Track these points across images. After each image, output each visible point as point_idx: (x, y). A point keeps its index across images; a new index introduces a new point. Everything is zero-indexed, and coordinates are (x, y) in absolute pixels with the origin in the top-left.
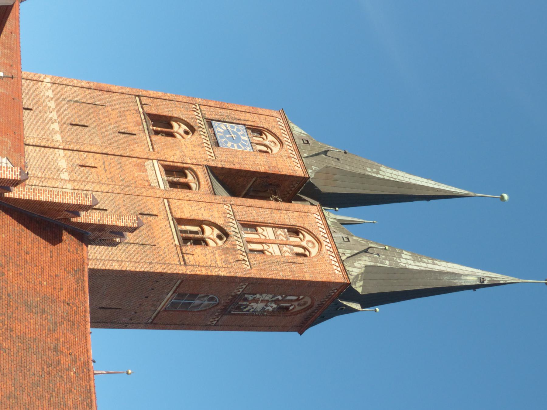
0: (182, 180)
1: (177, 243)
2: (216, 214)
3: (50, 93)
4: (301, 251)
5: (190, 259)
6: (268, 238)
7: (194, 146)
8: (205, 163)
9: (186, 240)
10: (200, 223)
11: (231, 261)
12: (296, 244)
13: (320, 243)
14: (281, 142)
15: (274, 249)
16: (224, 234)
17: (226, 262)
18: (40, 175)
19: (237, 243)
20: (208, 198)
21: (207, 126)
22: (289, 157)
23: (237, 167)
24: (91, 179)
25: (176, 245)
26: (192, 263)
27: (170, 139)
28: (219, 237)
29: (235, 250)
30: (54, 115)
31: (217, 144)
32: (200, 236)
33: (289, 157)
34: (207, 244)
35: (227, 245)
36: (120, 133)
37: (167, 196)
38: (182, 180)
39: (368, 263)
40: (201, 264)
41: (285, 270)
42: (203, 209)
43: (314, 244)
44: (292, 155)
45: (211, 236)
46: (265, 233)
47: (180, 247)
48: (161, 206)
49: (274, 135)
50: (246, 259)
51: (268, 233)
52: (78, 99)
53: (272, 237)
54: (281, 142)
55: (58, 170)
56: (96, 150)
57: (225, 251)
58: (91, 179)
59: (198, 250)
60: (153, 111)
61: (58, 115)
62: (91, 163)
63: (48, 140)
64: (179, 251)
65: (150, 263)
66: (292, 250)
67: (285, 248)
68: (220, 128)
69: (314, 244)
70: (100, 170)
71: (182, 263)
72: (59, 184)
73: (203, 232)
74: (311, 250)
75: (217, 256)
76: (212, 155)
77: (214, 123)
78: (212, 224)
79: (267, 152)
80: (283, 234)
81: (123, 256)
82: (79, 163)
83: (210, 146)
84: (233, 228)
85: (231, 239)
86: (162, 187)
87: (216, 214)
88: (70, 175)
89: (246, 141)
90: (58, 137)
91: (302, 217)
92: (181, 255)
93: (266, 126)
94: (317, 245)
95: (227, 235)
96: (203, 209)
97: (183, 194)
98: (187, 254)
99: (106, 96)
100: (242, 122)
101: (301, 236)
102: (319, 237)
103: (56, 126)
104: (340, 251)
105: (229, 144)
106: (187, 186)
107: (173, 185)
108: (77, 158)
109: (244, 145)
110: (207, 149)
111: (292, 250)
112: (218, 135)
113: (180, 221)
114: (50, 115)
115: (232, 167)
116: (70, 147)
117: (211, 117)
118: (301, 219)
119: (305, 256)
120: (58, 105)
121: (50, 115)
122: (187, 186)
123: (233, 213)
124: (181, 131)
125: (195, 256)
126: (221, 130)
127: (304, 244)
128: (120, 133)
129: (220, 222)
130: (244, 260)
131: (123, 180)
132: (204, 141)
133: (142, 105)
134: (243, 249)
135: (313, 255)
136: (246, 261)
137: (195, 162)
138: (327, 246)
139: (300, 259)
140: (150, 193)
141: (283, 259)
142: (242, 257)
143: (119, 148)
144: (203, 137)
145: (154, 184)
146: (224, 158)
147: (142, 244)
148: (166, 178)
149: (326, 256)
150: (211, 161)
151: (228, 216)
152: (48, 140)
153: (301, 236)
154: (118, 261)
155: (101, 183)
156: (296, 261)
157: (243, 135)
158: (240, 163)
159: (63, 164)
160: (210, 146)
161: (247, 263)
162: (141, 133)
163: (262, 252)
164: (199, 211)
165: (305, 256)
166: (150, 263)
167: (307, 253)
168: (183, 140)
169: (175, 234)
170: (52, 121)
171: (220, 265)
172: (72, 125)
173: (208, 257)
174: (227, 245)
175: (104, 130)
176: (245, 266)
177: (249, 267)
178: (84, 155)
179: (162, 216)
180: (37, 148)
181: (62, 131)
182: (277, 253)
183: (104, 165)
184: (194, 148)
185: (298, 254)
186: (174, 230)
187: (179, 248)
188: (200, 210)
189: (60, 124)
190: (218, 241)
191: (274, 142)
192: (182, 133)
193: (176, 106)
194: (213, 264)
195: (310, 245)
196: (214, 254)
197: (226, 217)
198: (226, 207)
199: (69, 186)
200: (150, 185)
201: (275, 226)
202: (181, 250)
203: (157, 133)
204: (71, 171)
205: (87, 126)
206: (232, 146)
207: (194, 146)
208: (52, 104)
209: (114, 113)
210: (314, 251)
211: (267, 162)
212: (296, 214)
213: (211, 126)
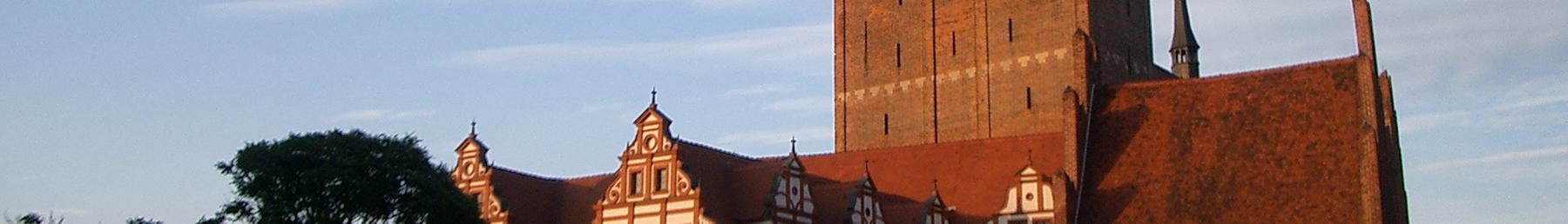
3: (860, 93)
18: (974, 103)
30: (890, 88)
55: (964, 80)
58: (971, 39)
62: (947, 39)
63: (925, 95)
70: (956, 27)
72: (984, 79)
88: (968, 66)
90: (920, 81)
99: (850, 21)
103: (905, 85)
108: (945, 57)
114: (890, 92)
121: (890, 92)
152: (925, 95)
159: (954, 75)
170: (898, 90)
175: (901, 24)
181: (911, 77)
204: (964, 65)
208: (874, 90)
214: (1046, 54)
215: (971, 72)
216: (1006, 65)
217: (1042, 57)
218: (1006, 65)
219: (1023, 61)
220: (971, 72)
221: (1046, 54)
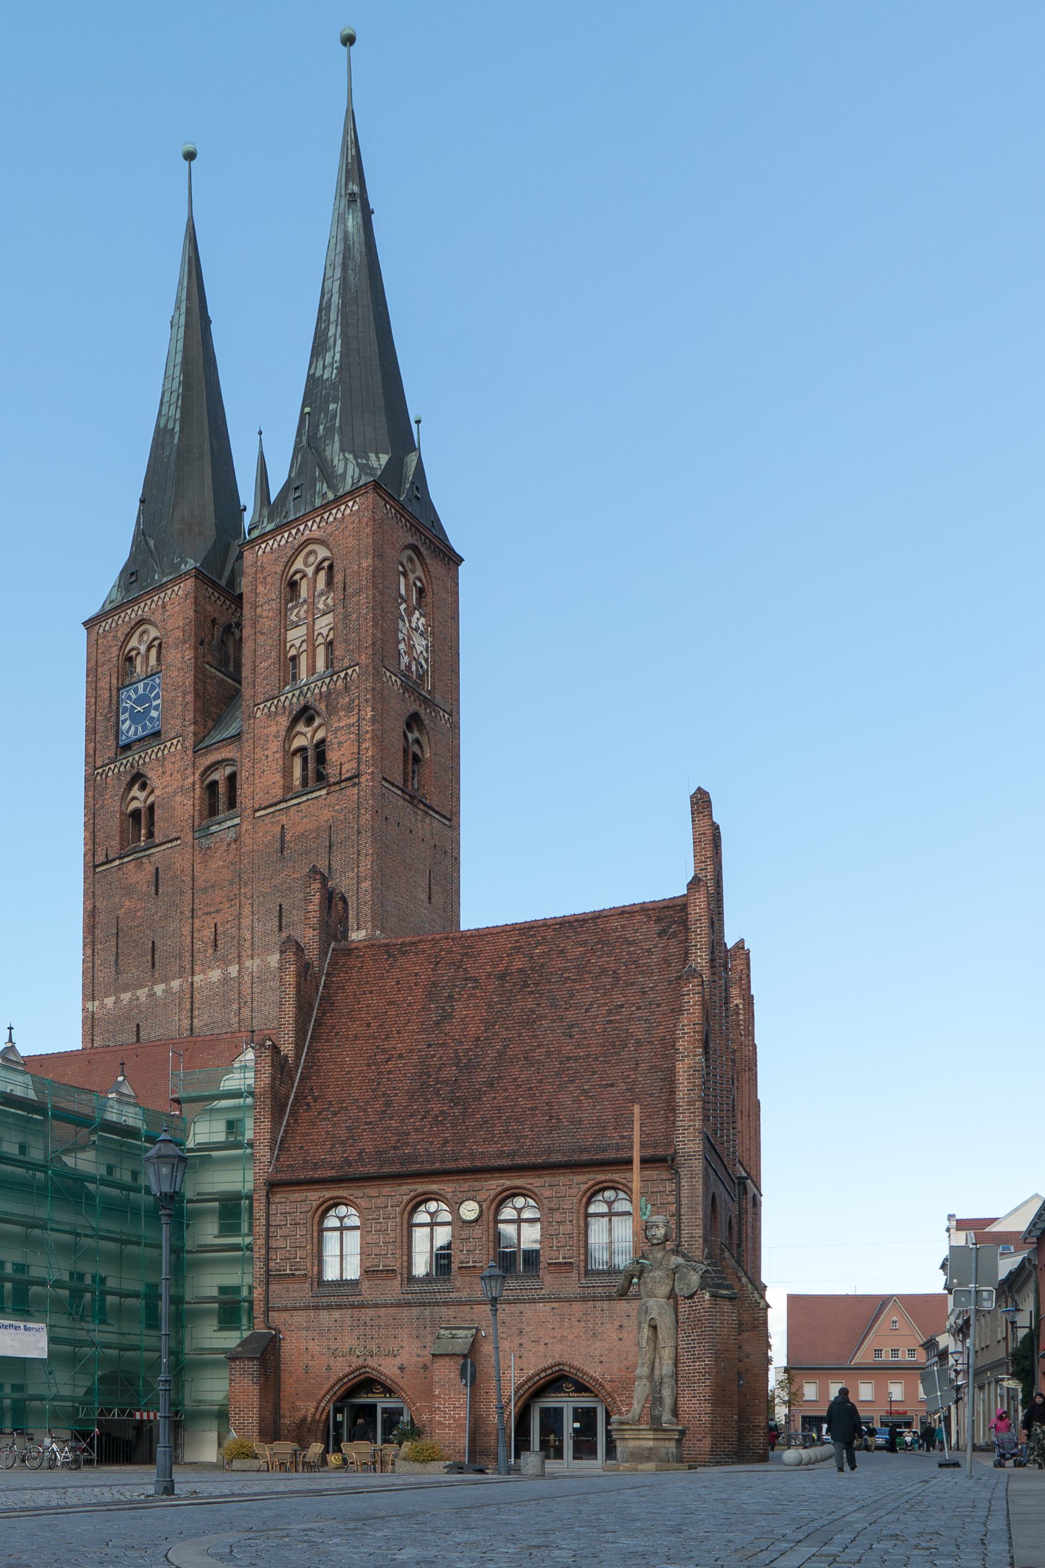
0: (222, 789)
1: (324, 792)
3: (109, 1001)
4: (322, 576)
6: (305, 637)
7: (164, 773)
8: (190, 752)
9: (321, 777)
10: (290, 754)
11: (347, 699)
12: (311, 585)
14: (141, 622)
15: (323, 624)
16: (305, 714)
17: (349, 708)
18: (235, 1007)
19: (317, 691)
20: (247, 746)
21: (129, 753)
23: (190, 698)
24: (234, 932)
25: (328, 794)
26: (355, 766)
27: (158, 812)
28: (310, 721)
30: (142, 993)
31: (157, 734)
32: (310, 753)
34: (323, 741)
35: (323, 706)
36: (157, 893)
37: (250, 811)
38: (222, 789)
39: (337, 445)
40: (356, 750)
41: (358, 603)
42: (266, 753)
43: (311, 553)
44: (160, 603)
45: (309, 736)
46: (297, 643)
47: (330, 786)
48: (267, 820)
49: (128, 636)
50: (342, 675)
51: (296, 636)
52: (113, 959)
53: (302, 631)
54: (141, 622)
55: (226, 980)
56: (186, 930)
57: (332, 710)
58: (234, 932)
59: (333, 756)
60: (115, 843)
61: (141, 986)
62: (208, 934)
63: (181, 998)
64: (337, 788)
66: (322, 594)
67: (321, 606)
68: (129, 730)
69: (311, 553)
70: (219, 918)
71: (356, 780)
73: (302, 749)
74: (319, 558)
75: (341, 724)
76: (175, 741)
77: (123, 740)
79: (160, 645)
80: (296, 611)
81: (350, 875)
82: (211, 951)
83: (162, 747)
84: (291, 699)
86: (237, 821)
87: (273, 729)
88: (231, 963)
89: (146, 686)
90: (175, 984)
91: (265, 578)
92: (343, 785)
93: (115, 651)
94: (310, 547)
95: (306, 709)
96: (266, 753)
97: (245, 786)
98: (340, 774)
99: (102, 918)
100: (114, 693)
101: (297, 577)
102: (297, 543)
103: (159, 989)
104: (318, 502)
105: (154, 714)
106: (232, 778)
109: (153, 688)
110: (166, 752)
111: (322, 594)
112: (141, 733)
113: (287, 788)
114: (143, 999)
115: (191, 707)
117: (113, 748)
118: (269, 579)
119: (331, 567)
120: (125, 991)
121: (143, 999)
122: (232, 778)
123: (268, 701)
124: (142, 795)
125: (344, 760)
126: (133, 729)
127: (310, 571)
128: (157, 893)
129: (284, 721)
130: (345, 678)
131: (232, 883)
132: (153, 756)
133: (108, 862)
134: (327, 680)
135: (329, 554)
136: (347, 674)
137: (190, 771)
138: (312, 529)
139: (338, 578)
140: (247, 839)
141: (340, 609)
142: (340, 682)
143: (182, 893)
144: (147, 759)
145: (232, 834)
146: (179, 722)
147: (330, 847)
148: (221, 816)
149: (330, 529)
150: (187, 744)
151: (273, 709)
152: (181, 998)
153: (297, 577)
154: (358, 883)
155: (239, 916)
156: (341, 585)
157: (136, 690)
158: (185, 693)
159: (215, 975)
160: (162, 747)
161: (350, 671)
162: (153, 859)
163: (330, 644)
164: (270, 759)
165: (331, 567)
166: (359, 833)
167: (326, 564)
168: (157, 792)
169: (310, 796)
170: (152, 995)
173: (343, 739)
174: (322, 707)
175: (156, 918)
176: (355, 674)
177: (357, 668)
178: (198, 945)
179: (284, 819)
180: (196, 1013)
181: (166, 980)
182: (329, 619)
183: (210, 913)
184: (168, 773)
185: (330, 582)
186: (304, 798)
187: (332, 788)
188: (267, 757)
189: (154, 984)
190: (316, 724)
191: (141, 635)
192: (145, 793)
193: (102, 807)
194: (354, 729)
195: (311, 559)
196: (337, 729)
197: (276, 712)
198: (259, 714)
199: (248, 963)
200: (235, 841)
201: (284, 625)
202: (335, 784)
203: (150, 835)
205: (153, 943)
206: (156, 708)
207: (164, 773)
208: (126, 997)
209: (127, 903)
210: (322, 552)
211: (176, 647)
212: (261, 589)
213: (127, 747)
215: (233, 970)
220: (233, 970)
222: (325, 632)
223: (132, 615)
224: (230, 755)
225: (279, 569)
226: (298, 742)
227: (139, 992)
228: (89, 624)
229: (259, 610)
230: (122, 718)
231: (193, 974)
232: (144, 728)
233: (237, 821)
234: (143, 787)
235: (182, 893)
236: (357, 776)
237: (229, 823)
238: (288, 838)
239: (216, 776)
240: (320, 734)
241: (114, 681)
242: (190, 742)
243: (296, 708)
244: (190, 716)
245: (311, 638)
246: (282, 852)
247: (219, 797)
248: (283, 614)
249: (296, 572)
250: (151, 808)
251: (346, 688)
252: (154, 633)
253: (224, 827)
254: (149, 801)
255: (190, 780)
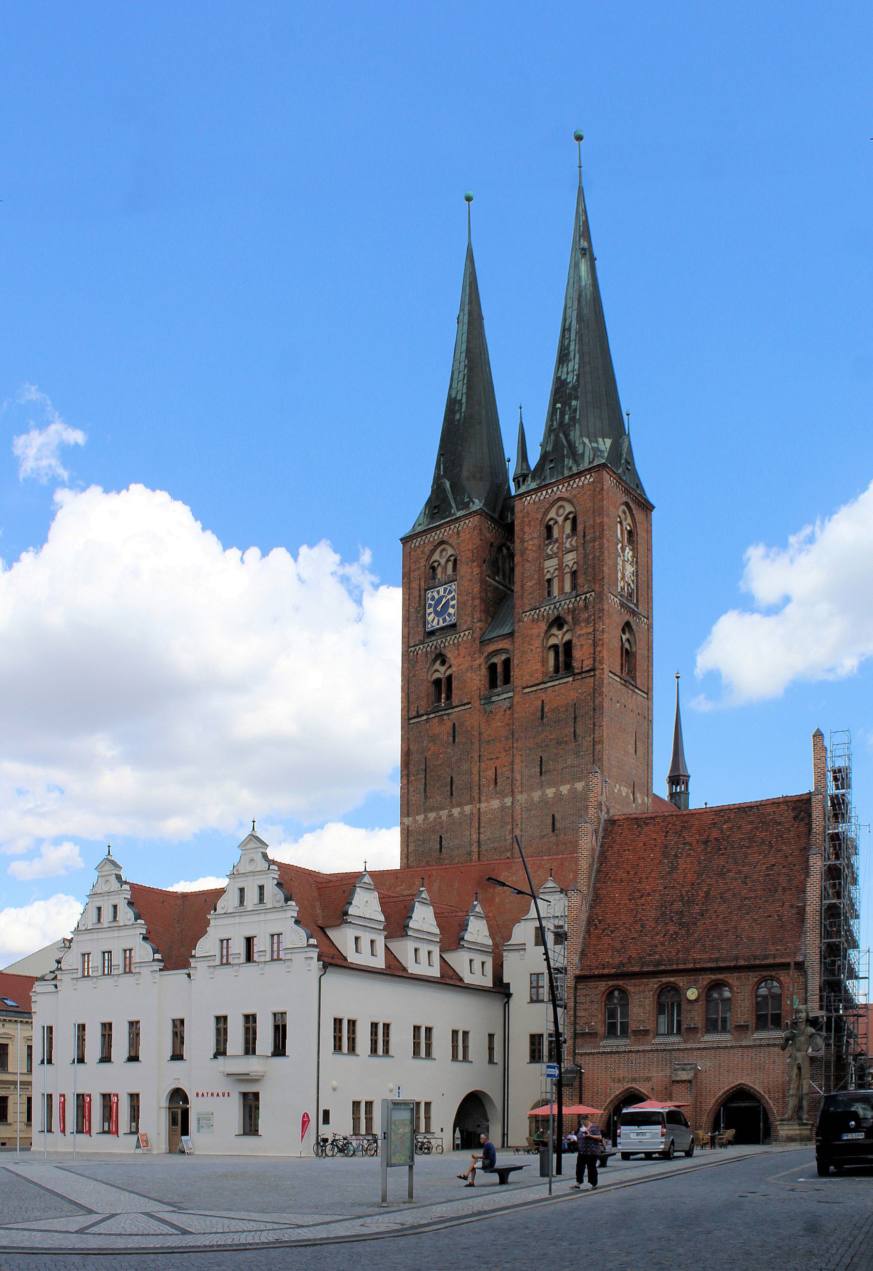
0: (500, 669)
1: (570, 679)
2: (535, 631)
5: (587, 664)
8: (477, 642)
11: (586, 615)
13: (560, 499)
14: (442, 542)
15: (570, 559)
16: (558, 622)
17: (587, 621)
18: (509, 827)
19: (566, 607)
20: (518, 640)
21: (433, 638)
22: (458, 533)
23: (477, 602)
27: (454, 684)
28: (560, 627)
29: (574, 610)
30: (444, 813)
31: (453, 626)
32: (561, 649)
33: (458, 533)
36: (454, 741)
37: (519, 688)
38: (500, 669)
43: (561, 507)
44: (455, 530)
45: (560, 637)
48: (532, 695)
49: (433, 552)
52: (422, 787)
53: (554, 562)
54: (442, 542)
55: (503, 808)
56: (475, 770)
58: (508, 774)
59: (577, 654)
61: (442, 809)
62: (491, 773)
65: (594, 710)
68: (434, 622)
69: (561, 507)
70: (498, 763)
73: (555, 647)
74: (567, 512)
75: (582, 632)
76: (467, 633)
77: (429, 628)
78: (548, 634)
79: (455, 560)
81: (588, 739)
82: (492, 786)
84: (549, 611)
85: (562, 614)
86: (511, 694)
89: (445, 589)
90: (467, 809)
91: (529, 522)
92: (584, 675)
93: (423, 562)
96: (531, 647)
97: (516, 670)
99: (415, 757)
100: (422, 593)
101: (551, 523)
103: (456, 811)
104: (566, 473)
105: (451, 611)
106: (507, 663)
107: (507, 680)
110: (460, 640)
112: (441, 624)
114: (444, 818)
115: (477, 609)
116: (476, 796)
118: (532, 523)
120: (432, 809)
121: (444, 818)
124: (442, 669)
126: (436, 621)
128: (454, 741)
129: (543, 626)
131: (507, 738)
132: (451, 642)
135: (573, 510)
138: (562, 490)
139: (580, 528)
143: (472, 743)
145: (507, 704)
146: (469, 619)
148: (499, 689)
149: (574, 492)
151: (536, 616)
154: (594, 745)
157: (438, 592)
158: (473, 599)
159: (495, 803)
160: (458, 636)
161: (588, 595)
162: (451, 717)
163: (574, 574)
165: (574, 520)
166: (594, 710)
167: (571, 516)
168: (454, 668)
170: (451, 815)
171: (590, 630)
172: (452, 795)
174: (569, 619)
177: (593, 593)
178: (484, 781)
179: (543, 695)
180: (482, 830)
181: (460, 805)
184: (462, 655)
186: (557, 682)
190: (565, 629)
193: (414, 676)
194: (591, 636)
195: (561, 511)
196: (580, 636)
197: (538, 619)
199: (519, 797)
200: (509, 708)
203: (449, 697)
204: (502, 795)
205: (452, 778)
206: (453, 607)
208: (432, 815)
210: (569, 508)
212: (527, 529)
213: (432, 633)
214: (568, 787)
215: (508, 801)
216: (536, 795)
217: (565, 789)
218: (536, 795)
219: (550, 792)
220: (508, 801)
221: (568, 787)
222: (570, 564)
223: (436, 536)
224: (505, 646)
225: (540, 516)
226: (553, 641)
227: (442, 813)
228: (405, 540)
229: (526, 544)
230: (428, 611)
231: (480, 802)
232: (444, 620)
233: (511, 694)
234: (443, 663)
235: (472, 743)
236: (593, 670)
237: (505, 696)
238: (546, 710)
239: (495, 660)
240: (567, 637)
241: (422, 584)
242: (477, 634)
243: (552, 618)
244: (477, 615)
245: (560, 568)
246: (542, 718)
247: (499, 675)
248: (541, 549)
249: (551, 519)
250: (449, 678)
251: (586, 607)
252: (450, 551)
253: (502, 697)
254: (447, 673)
255: (478, 662)
